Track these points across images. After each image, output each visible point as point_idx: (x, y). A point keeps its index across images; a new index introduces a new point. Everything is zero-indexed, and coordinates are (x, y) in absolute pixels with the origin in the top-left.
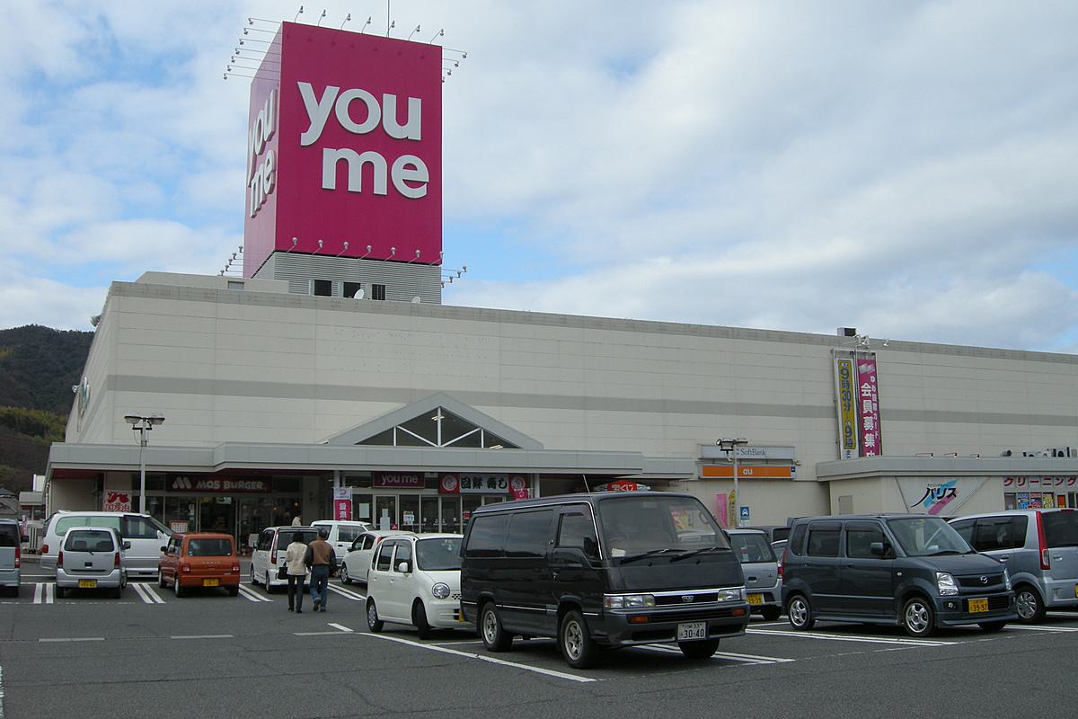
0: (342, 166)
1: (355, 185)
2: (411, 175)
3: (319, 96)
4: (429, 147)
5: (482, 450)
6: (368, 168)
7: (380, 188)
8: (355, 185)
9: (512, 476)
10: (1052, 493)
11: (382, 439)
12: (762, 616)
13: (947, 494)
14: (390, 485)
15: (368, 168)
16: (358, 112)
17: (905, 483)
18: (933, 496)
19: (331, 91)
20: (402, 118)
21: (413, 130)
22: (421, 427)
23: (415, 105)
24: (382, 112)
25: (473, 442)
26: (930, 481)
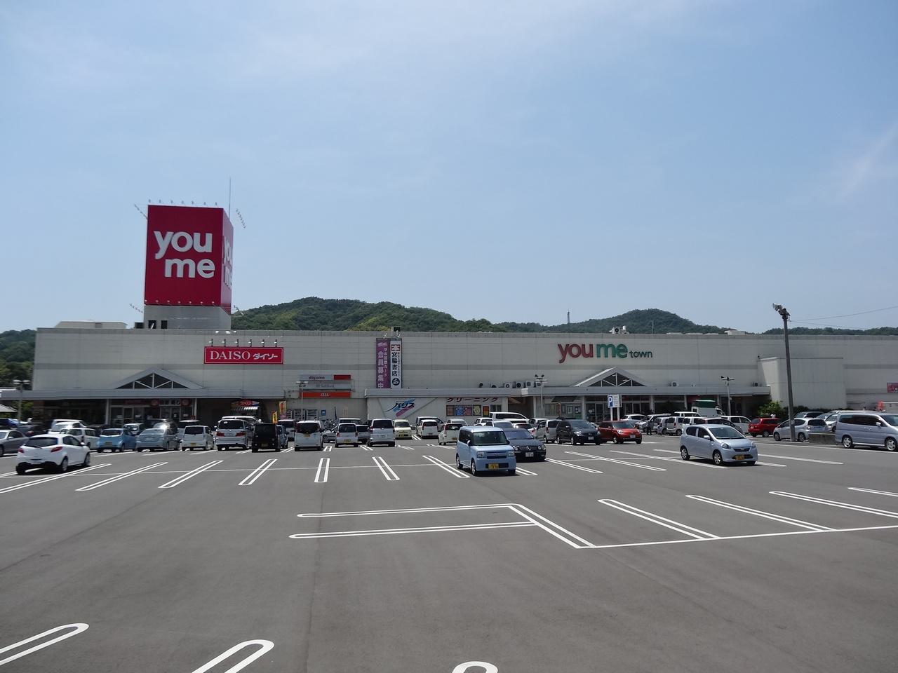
0: (174, 267)
1: (180, 274)
2: (207, 268)
3: (164, 236)
4: (217, 255)
5: (172, 389)
6: (186, 267)
7: (192, 275)
8: (180, 274)
9: (182, 399)
10: (480, 406)
11: (129, 386)
12: (322, 459)
13: (408, 406)
14: (129, 404)
15: (186, 267)
16: (182, 242)
17: (380, 400)
18: (399, 407)
19: (169, 234)
20: (203, 243)
21: (208, 248)
22: (146, 381)
23: (209, 237)
24: (193, 241)
25: (168, 386)
26: (398, 400)
